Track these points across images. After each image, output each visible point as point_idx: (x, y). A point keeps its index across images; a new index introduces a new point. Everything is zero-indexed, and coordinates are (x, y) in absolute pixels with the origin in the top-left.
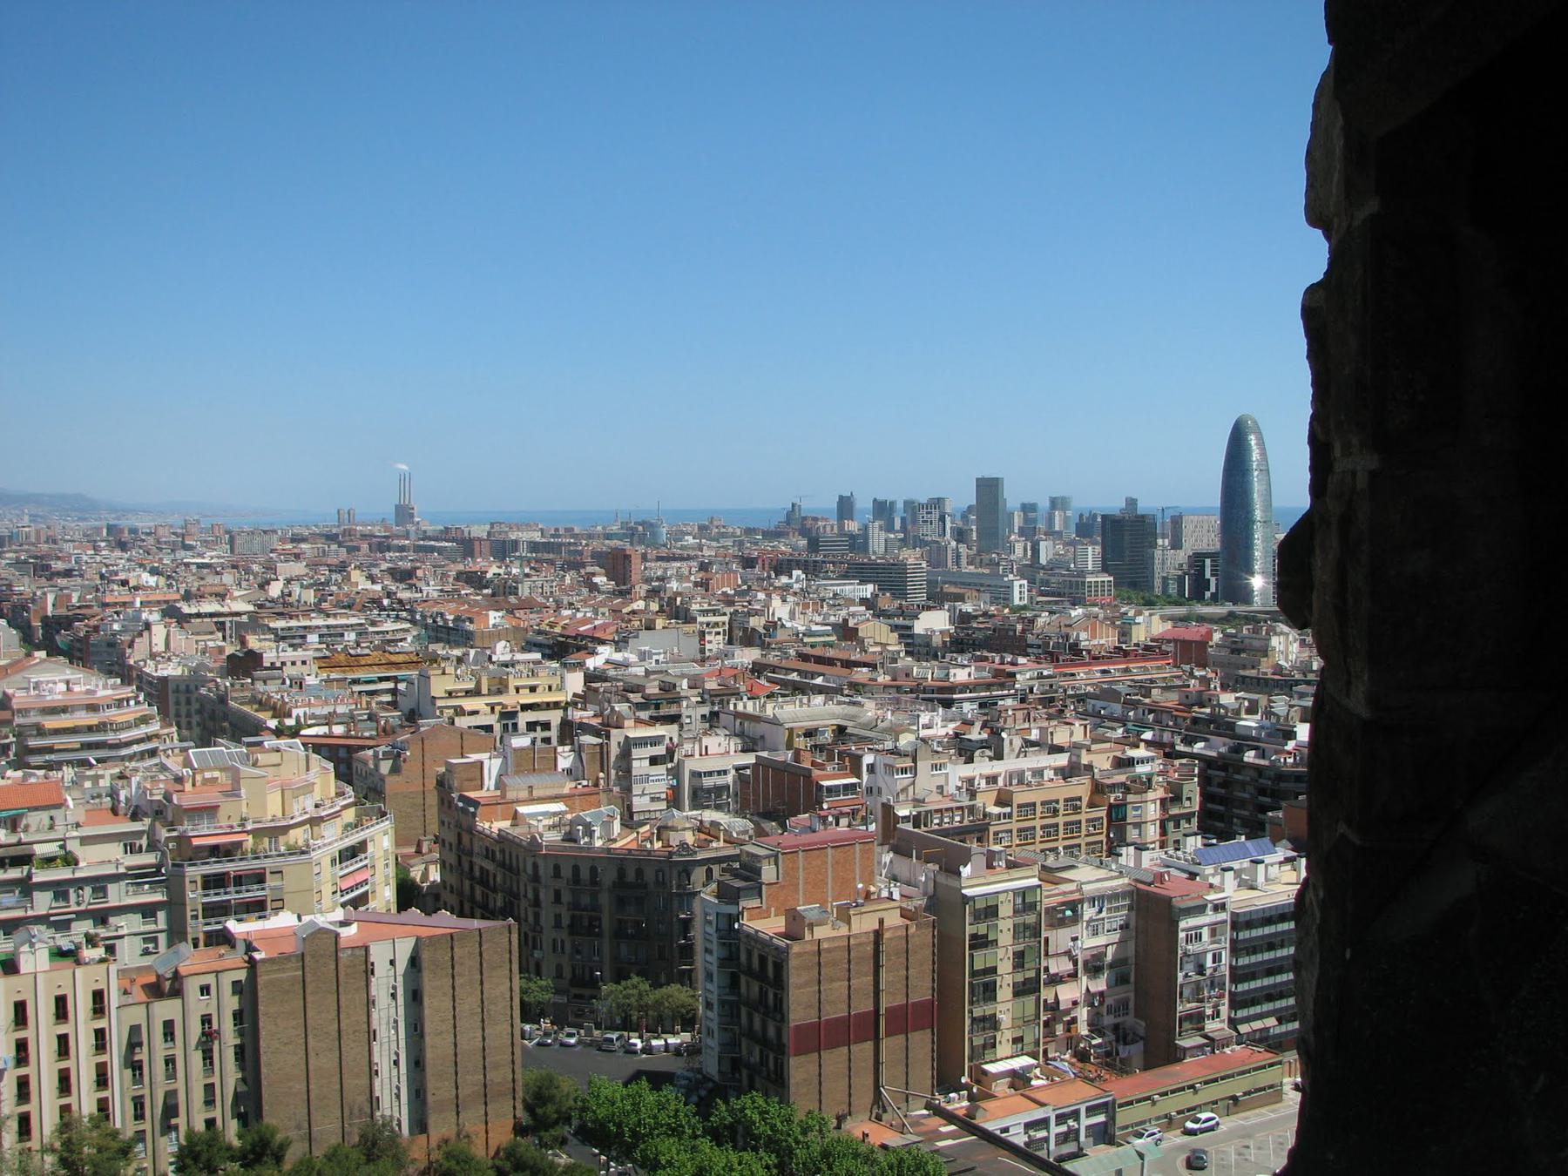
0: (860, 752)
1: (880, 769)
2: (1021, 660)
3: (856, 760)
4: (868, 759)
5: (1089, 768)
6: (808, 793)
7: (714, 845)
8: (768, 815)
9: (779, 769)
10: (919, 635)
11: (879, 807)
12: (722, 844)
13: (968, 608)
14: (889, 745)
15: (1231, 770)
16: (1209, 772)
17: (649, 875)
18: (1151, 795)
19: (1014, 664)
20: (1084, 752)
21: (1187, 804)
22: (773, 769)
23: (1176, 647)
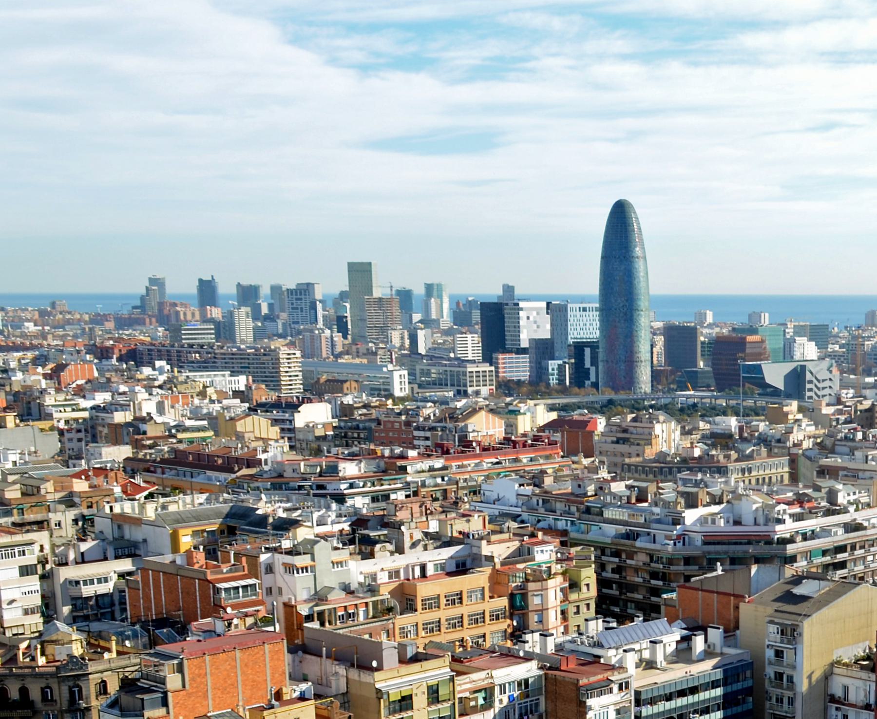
0: (254, 553)
1: (279, 569)
2: (412, 453)
3: (253, 559)
4: (264, 557)
5: (490, 559)
6: (205, 597)
7: (106, 655)
8: (161, 623)
9: (171, 573)
10: (300, 430)
11: (281, 606)
12: (114, 655)
13: (348, 400)
14: (286, 544)
15: (624, 556)
16: (604, 558)
17: (35, 694)
18: (551, 583)
19: (403, 457)
20: (484, 542)
21: (584, 589)
22: (164, 573)
23: (563, 436)
